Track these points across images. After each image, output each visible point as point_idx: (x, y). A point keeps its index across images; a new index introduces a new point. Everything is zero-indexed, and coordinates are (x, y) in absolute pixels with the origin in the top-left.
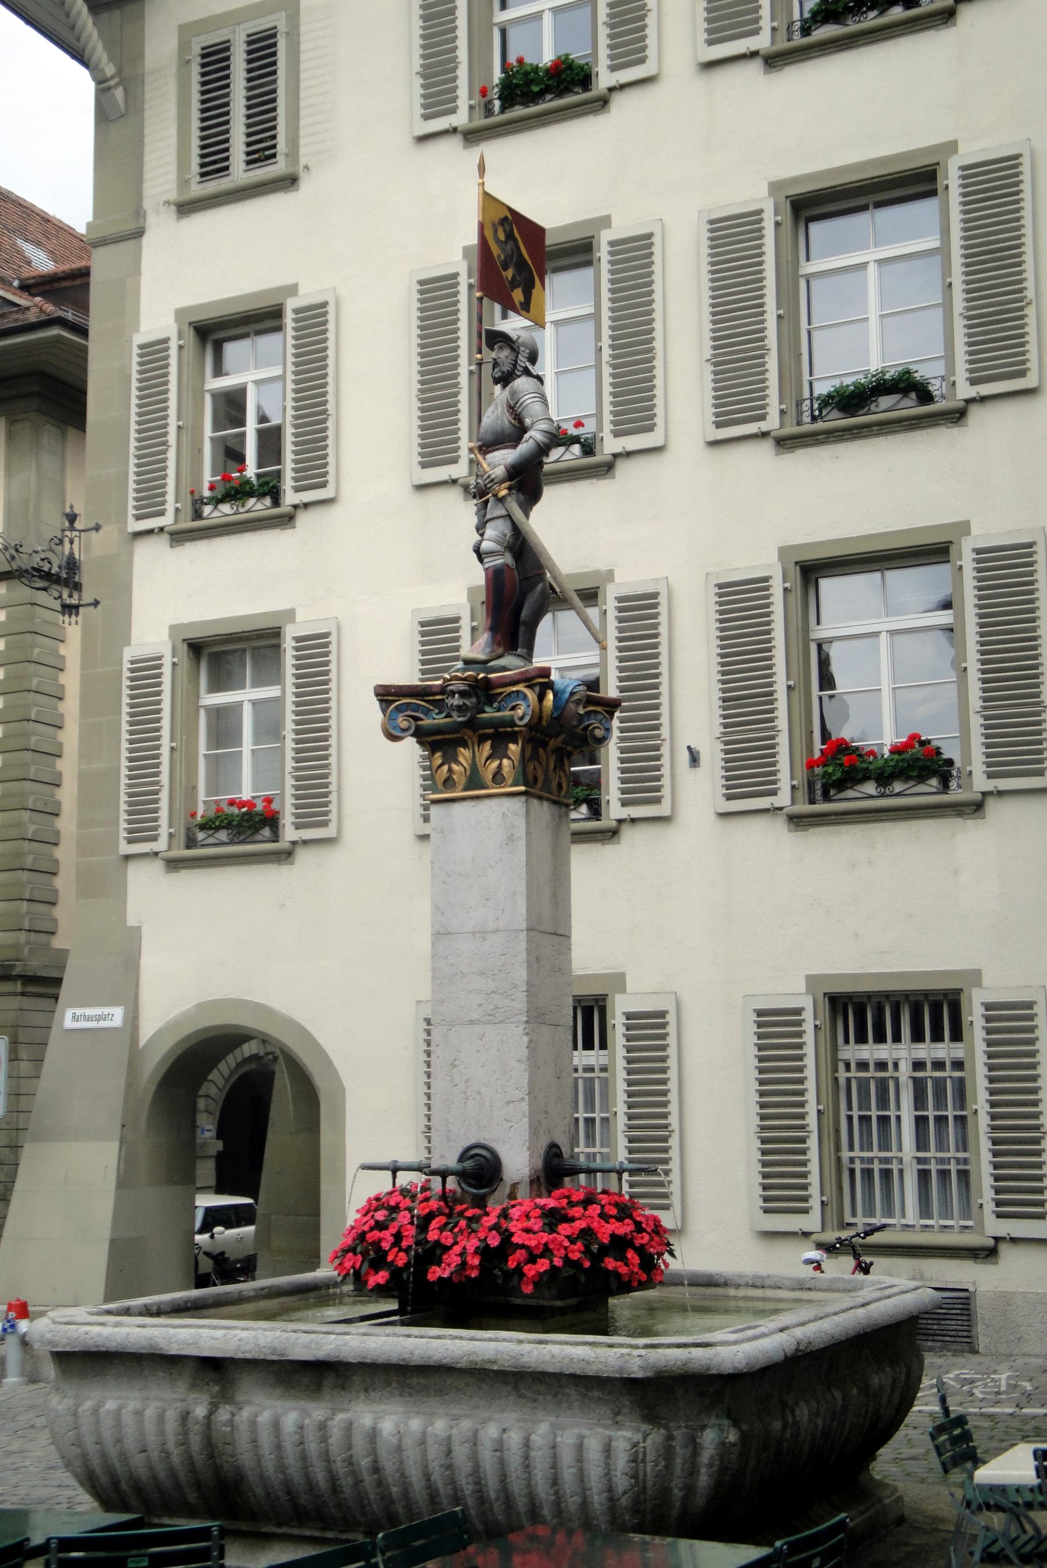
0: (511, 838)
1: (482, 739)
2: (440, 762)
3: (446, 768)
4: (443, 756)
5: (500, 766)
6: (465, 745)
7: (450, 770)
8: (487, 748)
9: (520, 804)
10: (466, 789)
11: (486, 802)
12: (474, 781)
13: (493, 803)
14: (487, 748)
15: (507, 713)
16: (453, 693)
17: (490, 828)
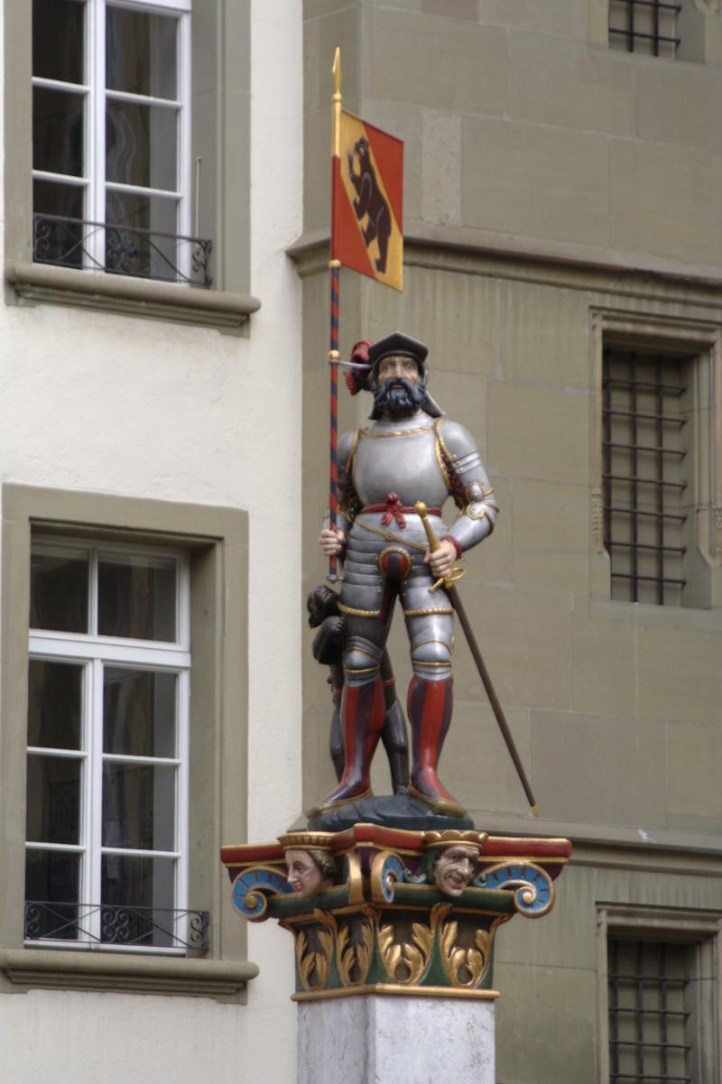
0: (477, 1059)
1: (448, 919)
2: (390, 939)
3: (398, 949)
4: (394, 932)
5: (465, 959)
6: (425, 920)
7: (403, 953)
8: (453, 927)
9: (489, 1014)
10: (425, 984)
11: (447, 1004)
12: (436, 976)
13: (458, 1007)
14: (453, 927)
15: (498, 890)
16: (459, 857)
17: (451, 1041)
